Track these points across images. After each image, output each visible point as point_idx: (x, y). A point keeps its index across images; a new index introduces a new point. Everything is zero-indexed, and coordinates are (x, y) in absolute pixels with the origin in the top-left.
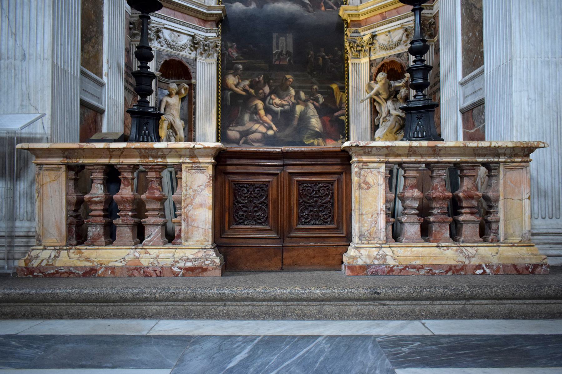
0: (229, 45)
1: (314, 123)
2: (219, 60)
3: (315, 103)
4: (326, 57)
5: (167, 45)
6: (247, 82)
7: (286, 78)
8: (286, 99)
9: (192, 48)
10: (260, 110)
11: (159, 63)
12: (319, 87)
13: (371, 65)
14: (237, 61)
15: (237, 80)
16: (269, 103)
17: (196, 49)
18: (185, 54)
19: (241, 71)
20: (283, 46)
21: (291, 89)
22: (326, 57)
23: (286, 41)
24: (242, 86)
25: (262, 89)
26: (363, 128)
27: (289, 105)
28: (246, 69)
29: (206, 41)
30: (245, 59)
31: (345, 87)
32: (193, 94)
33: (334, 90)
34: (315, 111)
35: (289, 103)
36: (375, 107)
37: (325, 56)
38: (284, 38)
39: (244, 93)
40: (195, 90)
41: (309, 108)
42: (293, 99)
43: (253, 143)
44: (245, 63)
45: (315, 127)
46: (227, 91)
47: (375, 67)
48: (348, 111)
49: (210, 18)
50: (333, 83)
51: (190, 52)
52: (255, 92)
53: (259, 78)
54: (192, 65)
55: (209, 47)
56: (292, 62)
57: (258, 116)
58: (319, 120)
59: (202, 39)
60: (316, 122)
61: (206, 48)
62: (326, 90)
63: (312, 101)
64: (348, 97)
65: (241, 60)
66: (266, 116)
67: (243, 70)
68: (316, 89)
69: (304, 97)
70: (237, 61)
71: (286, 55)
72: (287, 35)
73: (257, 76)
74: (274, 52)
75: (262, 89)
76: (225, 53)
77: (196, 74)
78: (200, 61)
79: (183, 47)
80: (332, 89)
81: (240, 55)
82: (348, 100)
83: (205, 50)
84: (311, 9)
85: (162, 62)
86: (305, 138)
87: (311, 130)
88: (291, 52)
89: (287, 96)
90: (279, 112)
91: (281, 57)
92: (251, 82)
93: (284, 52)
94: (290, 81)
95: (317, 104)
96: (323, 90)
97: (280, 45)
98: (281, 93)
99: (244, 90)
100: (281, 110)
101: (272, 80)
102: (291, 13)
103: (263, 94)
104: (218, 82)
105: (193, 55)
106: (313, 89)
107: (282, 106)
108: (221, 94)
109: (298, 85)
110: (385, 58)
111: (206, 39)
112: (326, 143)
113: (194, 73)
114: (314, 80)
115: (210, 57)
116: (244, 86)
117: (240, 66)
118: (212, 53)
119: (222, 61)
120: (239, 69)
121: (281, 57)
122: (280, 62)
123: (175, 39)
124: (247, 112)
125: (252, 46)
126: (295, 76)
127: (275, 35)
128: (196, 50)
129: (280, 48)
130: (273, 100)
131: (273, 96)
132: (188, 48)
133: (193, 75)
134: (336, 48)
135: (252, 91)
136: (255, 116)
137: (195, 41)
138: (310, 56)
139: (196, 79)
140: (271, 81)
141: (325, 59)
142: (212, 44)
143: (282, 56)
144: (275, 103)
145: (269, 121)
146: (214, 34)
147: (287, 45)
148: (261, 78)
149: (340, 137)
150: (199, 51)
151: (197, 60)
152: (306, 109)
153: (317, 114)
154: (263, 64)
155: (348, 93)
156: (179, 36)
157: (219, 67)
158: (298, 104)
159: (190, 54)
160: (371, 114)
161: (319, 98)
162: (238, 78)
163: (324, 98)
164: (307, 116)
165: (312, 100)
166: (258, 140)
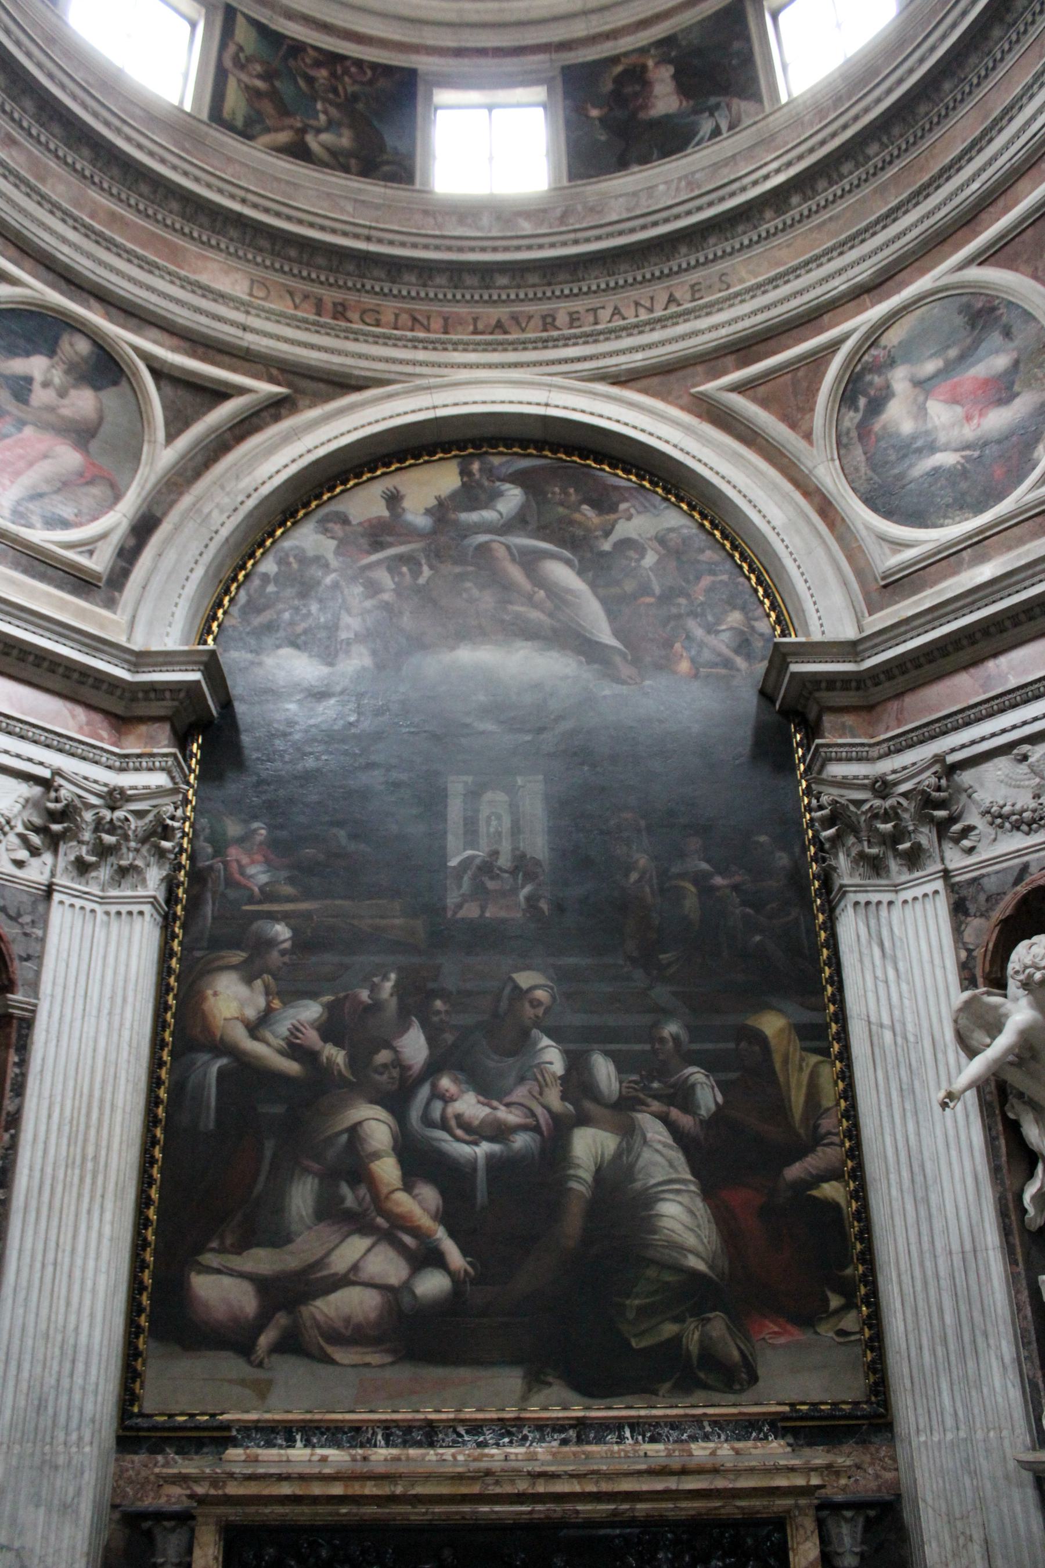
0: (233, 829)
1: (678, 1227)
2: (177, 901)
3: (675, 1113)
4: (718, 881)
6: (311, 1011)
7: (516, 987)
8: (520, 1094)
9: (35, 839)
10: (376, 1155)
12: (688, 1027)
13: (959, 909)
14: (266, 907)
15: (261, 1002)
16: (428, 1121)
17: (54, 842)
19: (283, 953)
20: (500, 834)
21: (546, 1041)
22: (718, 881)
23: (513, 807)
24: (283, 1028)
25: (388, 1045)
26: (956, 1247)
27: (536, 1129)
28: (303, 945)
29: (113, 809)
30: (308, 894)
31: (828, 1026)
32: (12, 1071)
33: (773, 1042)
34: (678, 1157)
35: (533, 1115)
36: (1014, 1129)
37: (710, 875)
38: (501, 797)
39: (292, 1067)
40: (23, 1047)
41: (645, 1142)
42: (553, 1097)
43: (329, 1349)
44: (308, 915)
45: (682, 1249)
46: (203, 1057)
47: (984, 915)
48: (856, 1152)
49: (142, 709)
50: (766, 1007)
51: (23, 854)
52: (352, 1061)
53: (374, 989)
54: (26, 919)
55: (126, 838)
56: (544, 905)
57: (363, 1191)
58: (700, 1206)
59: (94, 800)
60: (685, 1218)
61: (109, 839)
62: (732, 1045)
63: (656, 1106)
64: (847, 1076)
65: (289, 899)
66: (408, 1187)
67: (291, 951)
68: (676, 1039)
69: (615, 1086)
70: (266, 907)
71: (514, 872)
72: (520, 781)
73: (365, 979)
74: (453, 863)
75: (388, 1045)
76: (211, 868)
77: (40, 965)
78: (68, 900)
80: (760, 1039)
81: (284, 874)
82: (849, 1093)
83: (104, 852)
84: (626, 670)
86: (631, 1315)
87: (663, 1266)
88: (537, 863)
89: (522, 1080)
90: (481, 1163)
91: (491, 885)
92: (330, 1007)
93: (504, 861)
94: (536, 1003)
95: (686, 1121)
96: (709, 1046)
97: (483, 829)
98: (492, 1063)
99: (294, 1050)
100: (490, 1157)
101: (443, 994)
102: (537, 686)
103: (395, 1073)
104: (160, 1008)
105: (38, 871)
106: (662, 1040)
107: (499, 1132)
108: (170, 1072)
109: (578, 1019)
110: (1033, 869)
111: (115, 798)
112: (748, 1339)
113: (28, 958)
114: (662, 993)
115: (130, 880)
116: (295, 1031)
117: (282, 931)
118: (139, 863)
119: (194, 905)
120: (271, 943)
121: (491, 885)
122: (483, 909)
124: (307, 1170)
125: (342, 834)
126: (562, 976)
127: (457, 786)
128: (56, 852)
129: (483, 842)
130: (447, 1099)
131: (446, 1083)
132: (12, 838)
133: (20, 970)
134: (763, 838)
135: (336, 1056)
136: (345, 1189)
137: (51, 805)
138: (634, 876)
139: (34, 986)
140: (438, 1004)
141: (713, 889)
142: (140, 823)
143: (494, 877)
144: (458, 1117)
145: (425, 1221)
146: (160, 779)
147: (516, 829)
148: (388, 985)
149: (827, 1301)
150: (69, 851)
151: (57, 897)
152: (629, 1150)
153: (689, 1177)
154: (397, 922)
155: (845, 1055)
157: (174, 936)
158: (583, 1120)
159: (19, 864)
160: (995, 1171)
161: (693, 1086)
162: (267, 993)
163: (722, 1085)
164: (638, 1185)
165: (656, 1097)
166: (358, 1328)
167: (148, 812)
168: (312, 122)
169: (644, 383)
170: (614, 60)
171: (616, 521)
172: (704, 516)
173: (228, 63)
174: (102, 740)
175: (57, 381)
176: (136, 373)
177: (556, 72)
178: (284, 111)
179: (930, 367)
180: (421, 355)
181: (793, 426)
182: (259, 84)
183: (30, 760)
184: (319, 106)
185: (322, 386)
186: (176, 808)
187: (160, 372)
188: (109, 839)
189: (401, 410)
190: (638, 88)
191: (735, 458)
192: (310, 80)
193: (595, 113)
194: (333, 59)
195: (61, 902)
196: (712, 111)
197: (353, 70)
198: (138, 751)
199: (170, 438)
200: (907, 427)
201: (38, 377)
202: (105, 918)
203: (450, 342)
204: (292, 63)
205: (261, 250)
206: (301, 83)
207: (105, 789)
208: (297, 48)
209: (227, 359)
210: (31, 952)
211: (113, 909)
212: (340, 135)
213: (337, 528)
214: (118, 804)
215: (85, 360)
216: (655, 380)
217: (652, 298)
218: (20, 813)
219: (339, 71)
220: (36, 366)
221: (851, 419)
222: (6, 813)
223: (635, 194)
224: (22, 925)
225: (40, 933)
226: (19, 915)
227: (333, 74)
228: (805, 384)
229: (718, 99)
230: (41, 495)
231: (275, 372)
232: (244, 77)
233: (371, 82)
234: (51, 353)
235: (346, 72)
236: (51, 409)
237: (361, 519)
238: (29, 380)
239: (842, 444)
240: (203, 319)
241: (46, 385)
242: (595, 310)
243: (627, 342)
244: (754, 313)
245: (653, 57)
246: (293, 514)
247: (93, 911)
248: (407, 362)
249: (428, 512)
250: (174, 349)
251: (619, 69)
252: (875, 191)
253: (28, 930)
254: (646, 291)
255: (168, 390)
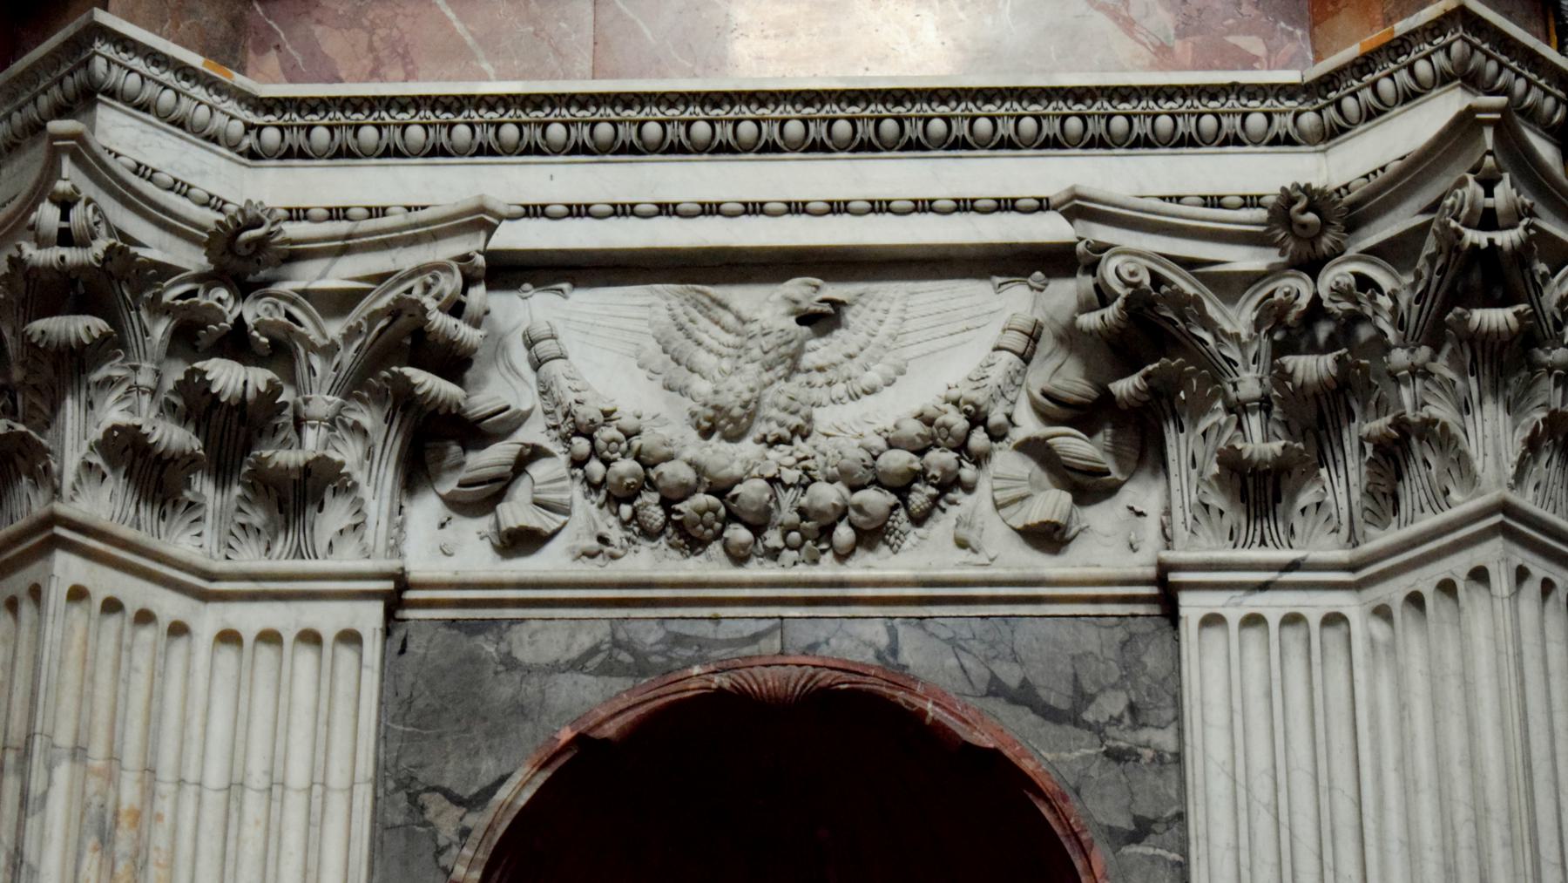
5: (616, 496)
9: (1076, 446)
11: (447, 820)
18: (952, 564)
51: (1051, 503)
61: (1310, 367)
78: (1234, 607)
79: (898, 460)
85: (518, 790)
113: (1142, 830)
118: (1441, 410)
123: (736, 388)
128: (1160, 465)
132: (1008, 463)
151: (1192, 606)
156: (822, 320)
159: (1047, 537)
167: (1421, 231)
174: (1249, 62)
183: (1006, 205)
186: (1489, 185)
188: (1310, 367)
195: (1212, 620)
198: (1352, 52)
202: (1379, 629)
207: (1261, 214)
210: (1146, 809)
211: (1394, 592)
214: (1326, 242)
218: (1015, 379)
222: (966, 392)
224: (1097, 730)
225: (1165, 739)
226: (1083, 698)
247: (1333, 619)
253: (1123, 739)
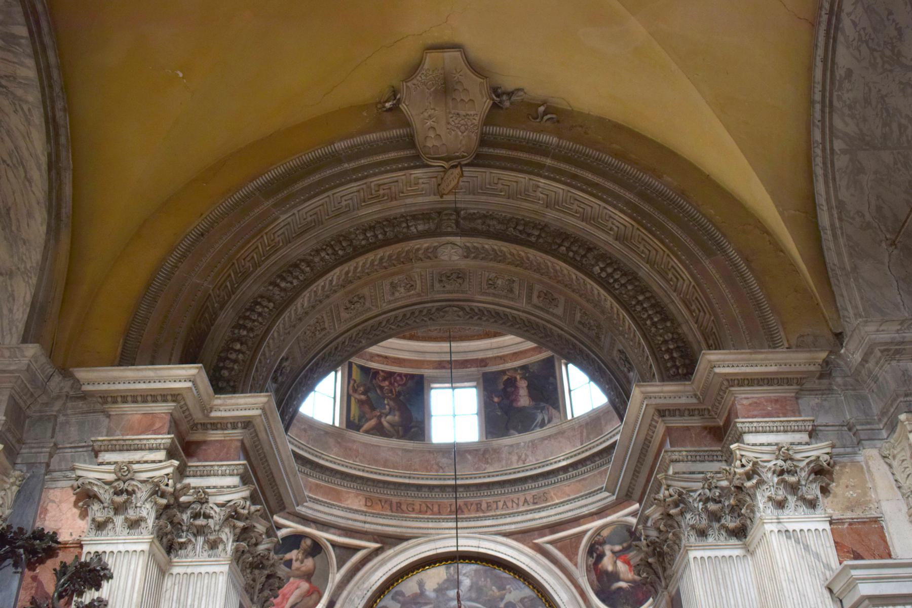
168: (383, 411)
169: (516, 536)
170: (504, 372)
171: (505, 594)
172: (539, 592)
173: (351, 392)
175: (300, 558)
176: (327, 548)
177: (480, 376)
178: (373, 408)
179: (618, 548)
180: (431, 525)
181: (571, 560)
182: (363, 397)
184: (386, 402)
185: (393, 540)
187: (334, 545)
189: (424, 550)
190: (513, 389)
191: (550, 571)
192: (381, 388)
193: (496, 400)
194: (390, 375)
196: (542, 409)
197: (398, 378)
199: (339, 568)
200: (610, 568)
201: (294, 558)
203: (441, 518)
204: (374, 381)
205: (369, 485)
206: (378, 391)
208: (376, 373)
209: (358, 535)
212: (395, 416)
213: (400, 598)
215: (309, 547)
216: (520, 536)
217: (518, 499)
219: (393, 381)
220: (293, 554)
221: (591, 561)
223: (512, 446)
227: (391, 383)
228: (574, 545)
229: (545, 405)
230: (297, 604)
231: (376, 537)
232: (357, 396)
233: (405, 384)
234: (298, 547)
235: (395, 381)
236: (298, 569)
237: (410, 594)
238: (291, 561)
239: (588, 571)
240: (350, 522)
241: (297, 560)
242: (497, 502)
243: (508, 520)
244: (556, 515)
245: (519, 374)
246: (384, 593)
248: (426, 528)
249: (436, 590)
250: (340, 535)
251: (506, 377)
252: (599, 473)
254: (516, 495)
255: (338, 551)
